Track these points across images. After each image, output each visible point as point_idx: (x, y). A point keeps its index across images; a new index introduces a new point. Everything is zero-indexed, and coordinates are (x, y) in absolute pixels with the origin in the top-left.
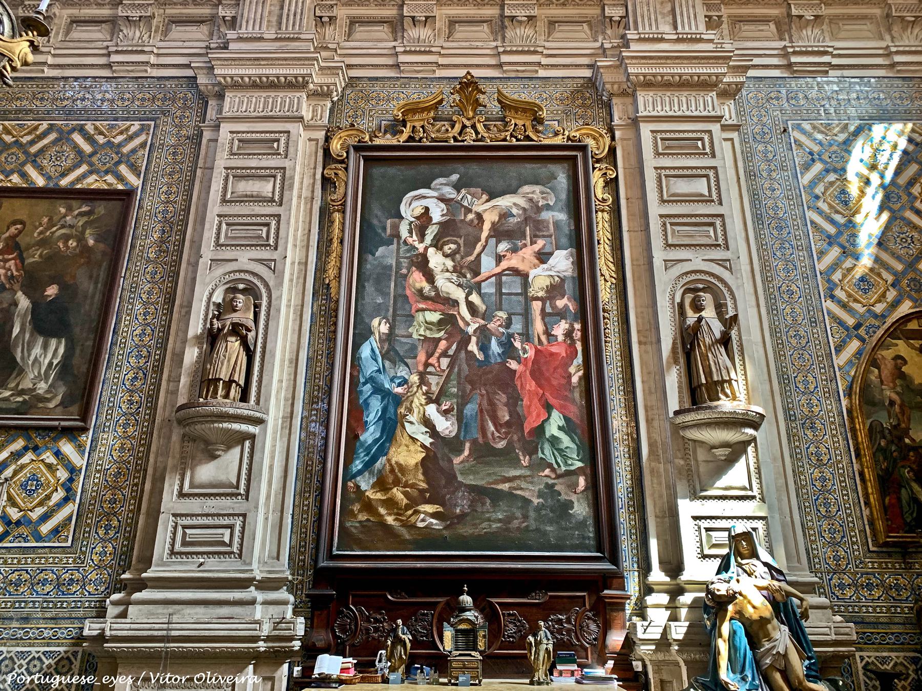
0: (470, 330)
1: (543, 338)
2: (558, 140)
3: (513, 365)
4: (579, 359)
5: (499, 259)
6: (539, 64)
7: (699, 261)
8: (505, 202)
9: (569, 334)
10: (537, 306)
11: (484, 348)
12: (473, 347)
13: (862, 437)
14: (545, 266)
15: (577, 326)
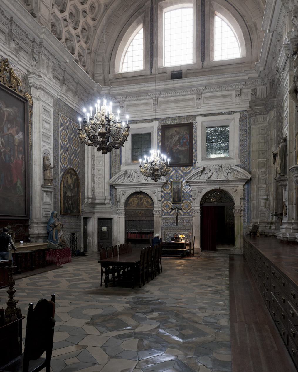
0: (2, 151)
1: (17, 158)
2: (21, 95)
3: (11, 164)
4: (24, 166)
5: (8, 129)
6: (18, 63)
7: (47, 147)
8: (9, 110)
9: (22, 158)
10: (16, 147)
11: (5, 157)
12: (3, 156)
13: (62, 193)
14: (18, 135)
15: (24, 156)
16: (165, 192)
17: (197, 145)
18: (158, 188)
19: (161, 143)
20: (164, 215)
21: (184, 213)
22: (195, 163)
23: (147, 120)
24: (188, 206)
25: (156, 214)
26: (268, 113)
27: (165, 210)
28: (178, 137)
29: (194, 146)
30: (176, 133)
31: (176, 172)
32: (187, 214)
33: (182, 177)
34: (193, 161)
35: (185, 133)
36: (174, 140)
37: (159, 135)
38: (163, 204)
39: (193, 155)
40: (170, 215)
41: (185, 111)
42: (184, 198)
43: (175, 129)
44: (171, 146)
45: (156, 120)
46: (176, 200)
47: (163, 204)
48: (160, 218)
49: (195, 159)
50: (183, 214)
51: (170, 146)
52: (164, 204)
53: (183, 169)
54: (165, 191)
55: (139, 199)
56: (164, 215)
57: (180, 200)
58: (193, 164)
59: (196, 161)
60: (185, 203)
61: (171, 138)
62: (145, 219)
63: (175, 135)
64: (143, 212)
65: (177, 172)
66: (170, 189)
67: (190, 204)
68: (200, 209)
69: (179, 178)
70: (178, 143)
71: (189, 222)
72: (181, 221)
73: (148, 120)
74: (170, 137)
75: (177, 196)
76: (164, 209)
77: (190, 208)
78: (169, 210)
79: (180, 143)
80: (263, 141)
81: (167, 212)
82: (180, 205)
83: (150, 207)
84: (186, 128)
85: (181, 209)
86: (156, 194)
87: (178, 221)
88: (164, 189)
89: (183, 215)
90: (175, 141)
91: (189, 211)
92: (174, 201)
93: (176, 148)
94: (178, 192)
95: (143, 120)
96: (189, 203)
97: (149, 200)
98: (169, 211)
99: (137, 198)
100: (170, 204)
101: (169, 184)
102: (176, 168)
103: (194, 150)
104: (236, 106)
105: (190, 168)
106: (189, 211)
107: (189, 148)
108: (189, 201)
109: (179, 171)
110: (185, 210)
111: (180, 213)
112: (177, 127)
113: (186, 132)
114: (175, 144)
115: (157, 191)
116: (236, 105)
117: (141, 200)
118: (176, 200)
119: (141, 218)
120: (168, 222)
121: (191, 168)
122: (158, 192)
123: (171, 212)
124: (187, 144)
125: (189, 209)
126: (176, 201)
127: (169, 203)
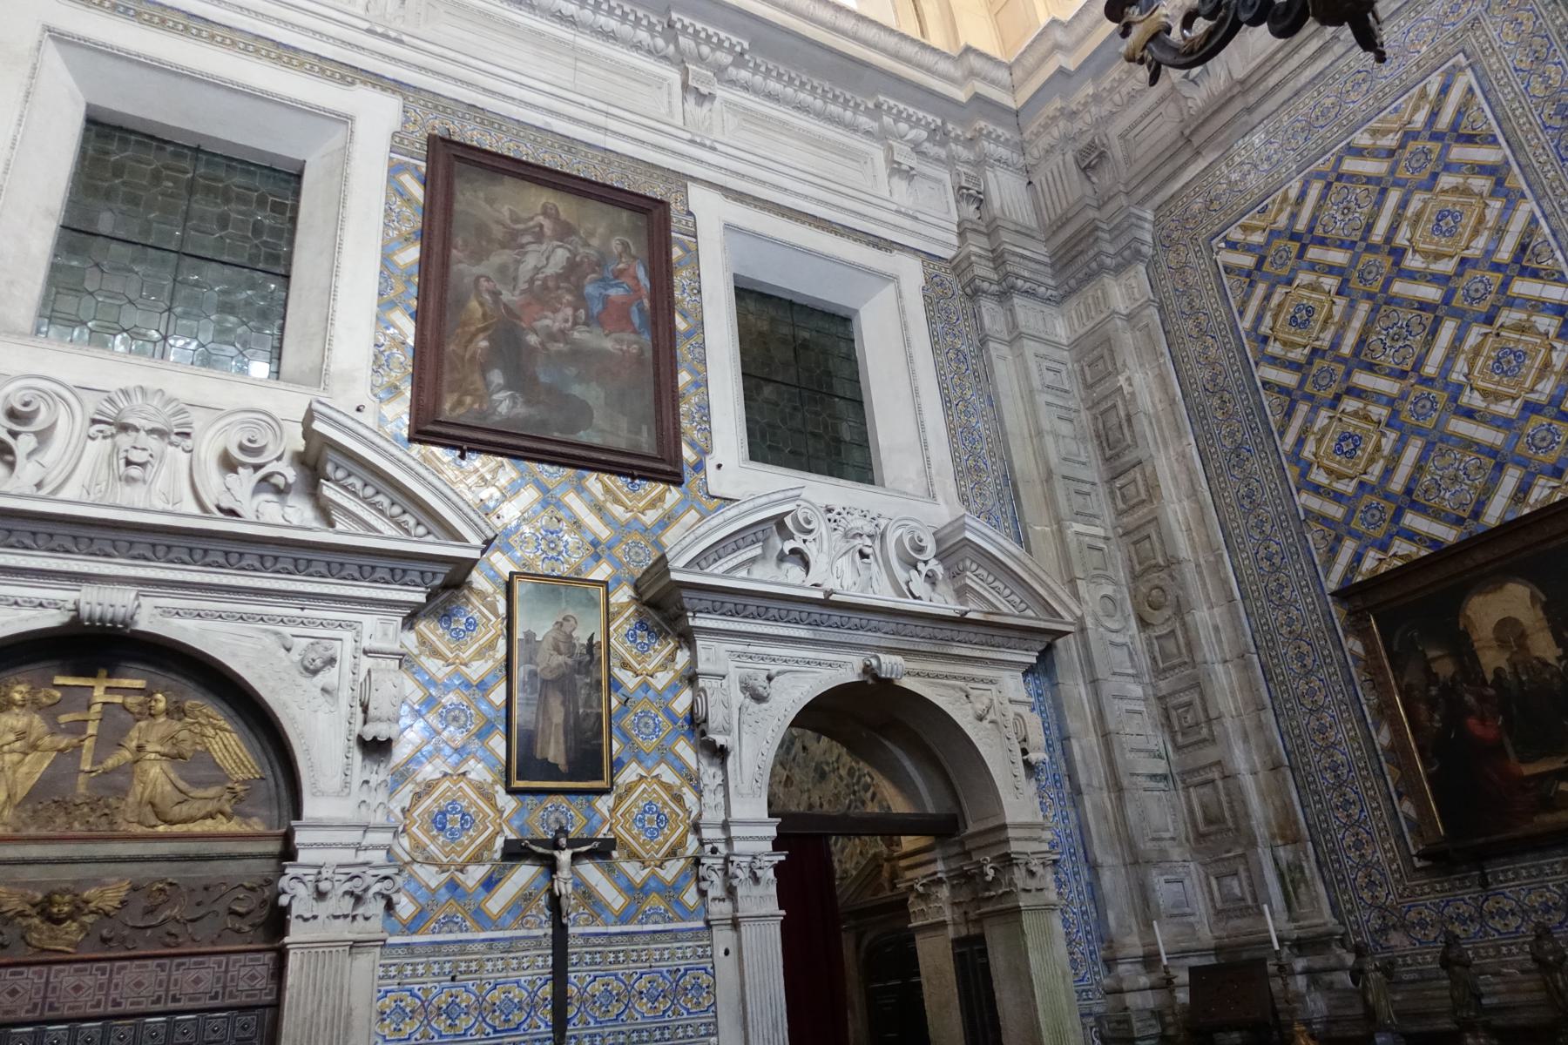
16: (434, 666)
17: (702, 345)
18: (370, 622)
19: (412, 254)
20: (412, 926)
21: (629, 888)
22: (699, 467)
23: (295, 50)
24: (662, 820)
25: (323, 909)
26: (1064, 297)
27: (430, 860)
28: (561, 255)
29: (683, 351)
30: (548, 225)
31: (545, 504)
32: (655, 901)
33: (597, 550)
34: (688, 454)
35: (615, 246)
36: (531, 261)
37: (395, 189)
38: (405, 795)
39: (683, 408)
40: (481, 918)
41: (613, 124)
42: (626, 737)
43: (538, 199)
44: (506, 296)
45: (377, 81)
46: (554, 751)
47: (405, 795)
48: (365, 966)
49: (697, 436)
50: (615, 899)
51: (496, 294)
52: (418, 796)
53: (607, 490)
54: (435, 653)
55: (78, 728)
56: (412, 926)
57: (588, 764)
58: (688, 474)
59: (704, 452)
60: (629, 789)
61: (503, 246)
62: (137, 984)
63: (539, 237)
64: (109, 896)
65: (548, 500)
66: (491, 646)
67: (678, 799)
68: (777, 845)
69: (575, 558)
70: (569, 297)
71: (677, 992)
72: (597, 987)
73: (302, 57)
74: (498, 232)
75: (558, 716)
76: (418, 846)
77: (681, 843)
78: (477, 859)
79: (581, 300)
80: (1065, 428)
81: (453, 886)
82: (591, 807)
83: (233, 826)
84: (625, 216)
85: (602, 851)
86: (328, 677)
87: (572, 990)
88: (423, 641)
89: (623, 918)
90: (537, 270)
91: (671, 871)
92: (526, 770)
93: (552, 322)
94: (561, 683)
95: (258, 37)
96: (667, 787)
97: (228, 744)
98: (475, 875)
99: (49, 711)
100: (489, 798)
101: (482, 595)
102: (546, 472)
103: (684, 377)
104: (899, 220)
105: (660, 498)
106: (671, 871)
107: (649, 354)
108: (669, 776)
109: (572, 500)
110: (633, 856)
111: (587, 894)
112: (555, 186)
113: (625, 246)
114: (541, 294)
115: (345, 650)
116: (898, 212)
117: (112, 738)
118: (554, 751)
119: (66, 977)
120: (450, 1011)
121: (673, 495)
122: (366, 663)
123: (489, 884)
124: (636, 320)
125: (672, 854)
126: (550, 771)
127: (480, 789)
